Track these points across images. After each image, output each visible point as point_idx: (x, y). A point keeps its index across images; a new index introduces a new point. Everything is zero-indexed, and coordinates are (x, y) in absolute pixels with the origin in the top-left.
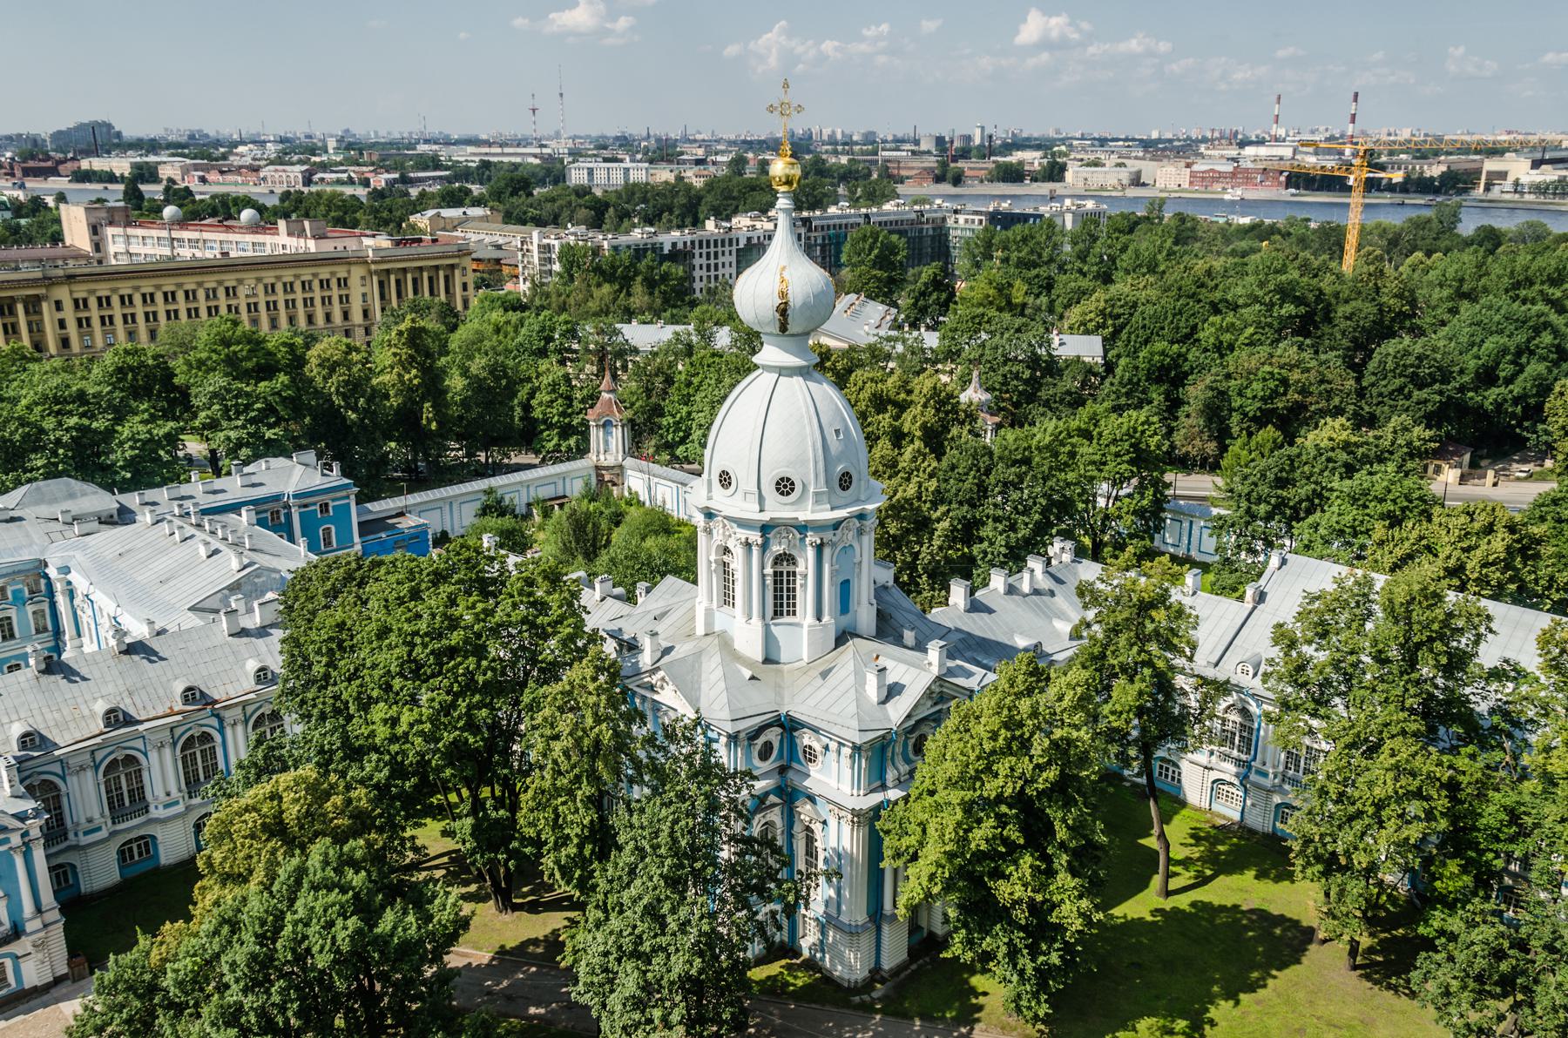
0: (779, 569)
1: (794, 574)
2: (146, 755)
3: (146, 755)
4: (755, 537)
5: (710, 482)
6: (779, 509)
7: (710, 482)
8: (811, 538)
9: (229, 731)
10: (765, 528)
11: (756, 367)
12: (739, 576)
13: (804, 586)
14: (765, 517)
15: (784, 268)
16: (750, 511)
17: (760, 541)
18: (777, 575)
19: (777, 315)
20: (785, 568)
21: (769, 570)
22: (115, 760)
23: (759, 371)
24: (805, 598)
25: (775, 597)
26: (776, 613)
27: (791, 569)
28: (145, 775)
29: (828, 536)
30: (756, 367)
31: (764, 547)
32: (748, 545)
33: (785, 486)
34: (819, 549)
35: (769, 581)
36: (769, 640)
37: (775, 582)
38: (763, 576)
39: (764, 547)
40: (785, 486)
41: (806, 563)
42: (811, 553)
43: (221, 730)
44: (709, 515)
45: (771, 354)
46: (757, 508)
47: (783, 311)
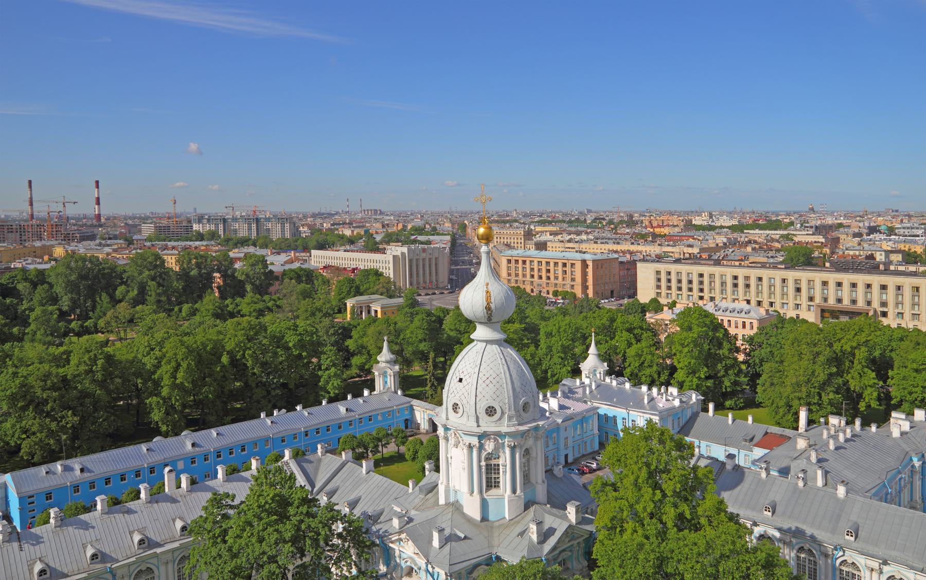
1: (498, 465)
4: (475, 441)
5: (447, 409)
6: (489, 425)
7: (447, 409)
10: (482, 437)
11: (473, 341)
13: (505, 472)
14: (481, 430)
15: (487, 284)
16: (471, 425)
17: (477, 445)
18: (488, 467)
21: (483, 463)
23: (475, 342)
24: (505, 479)
30: (473, 341)
31: (481, 447)
32: (470, 447)
33: (490, 411)
34: (513, 449)
36: (484, 504)
37: (487, 469)
38: (480, 467)
40: (490, 411)
41: (505, 459)
42: (507, 451)
44: (447, 429)
45: (481, 332)
46: (476, 425)
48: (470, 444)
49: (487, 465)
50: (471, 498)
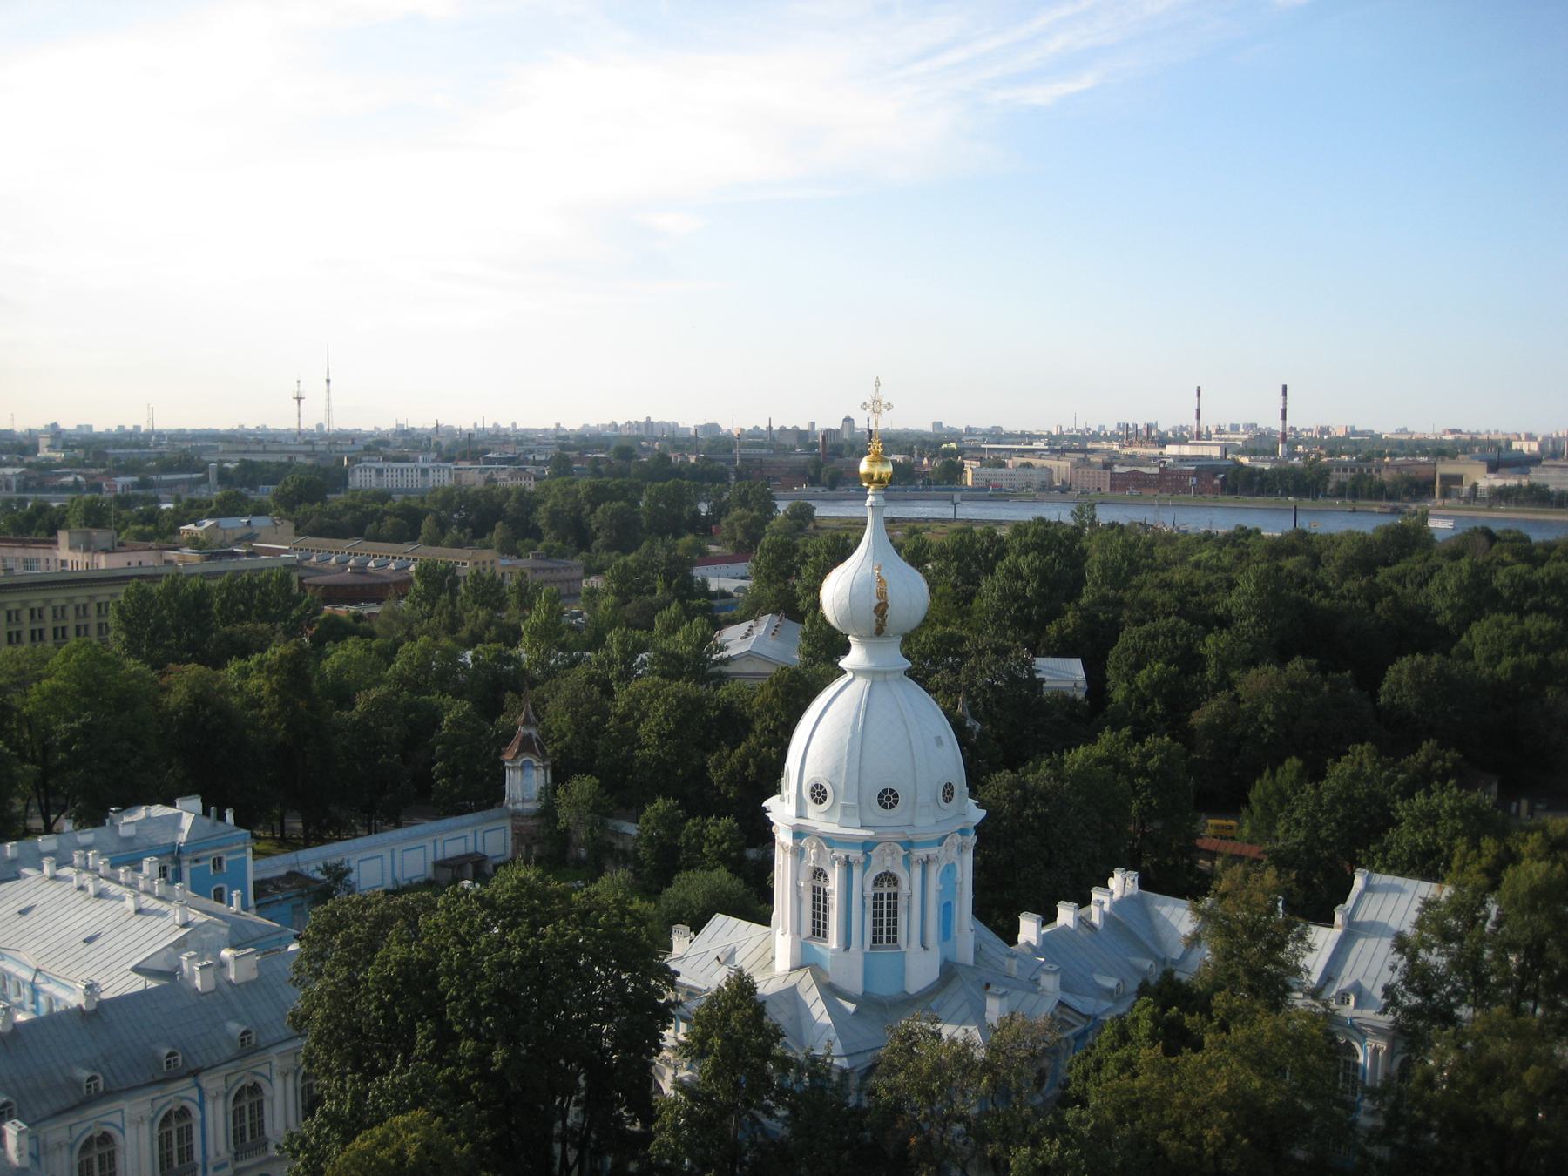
0: (879, 890)
1: (896, 896)
2: (270, 1081)
3: (122, 1132)
4: (856, 854)
8: (919, 853)
9: (209, 1106)
10: (867, 846)
11: (844, 672)
12: (835, 900)
13: (909, 907)
17: (862, 860)
18: (877, 897)
19: (874, 617)
20: (886, 889)
21: (870, 891)
22: (91, 1137)
25: (875, 923)
26: (874, 940)
27: (892, 890)
28: (266, 1106)
29: (933, 851)
30: (844, 672)
33: (888, 799)
35: (869, 903)
37: (875, 906)
39: (866, 866)
41: (909, 883)
42: (917, 871)
43: (201, 1106)
47: (881, 610)
48: (847, 857)
49: (875, 897)
50: (845, 955)
